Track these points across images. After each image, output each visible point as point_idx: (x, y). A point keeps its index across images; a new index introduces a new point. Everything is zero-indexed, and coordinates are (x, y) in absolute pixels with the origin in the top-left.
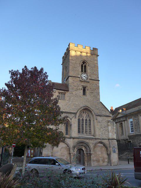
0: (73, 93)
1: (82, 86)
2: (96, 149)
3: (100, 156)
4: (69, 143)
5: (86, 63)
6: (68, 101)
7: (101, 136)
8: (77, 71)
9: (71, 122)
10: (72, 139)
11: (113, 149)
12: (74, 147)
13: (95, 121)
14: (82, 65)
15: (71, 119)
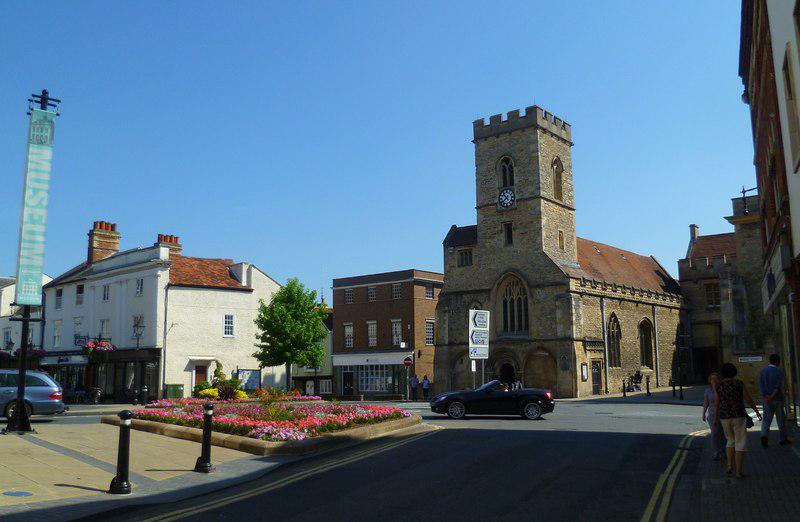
3: (543, 377)
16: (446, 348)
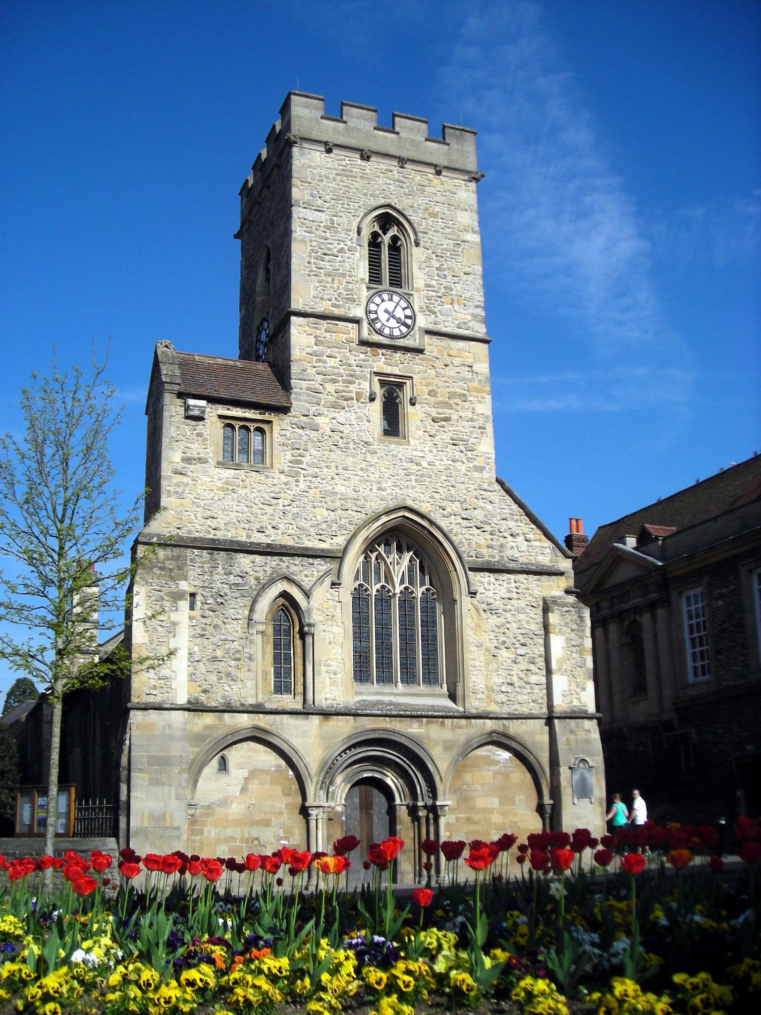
0: (320, 420)
1: (377, 374)
2: (468, 777)
4: (296, 742)
5: (399, 224)
6: (283, 478)
7: (502, 698)
8: (343, 275)
9: (309, 611)
10: (315, 720)
11: (576, 777)
12: (329, 772)
13: (465, 604)
14: (375, 235)
15: (307, 595)
16: (178, 717)
